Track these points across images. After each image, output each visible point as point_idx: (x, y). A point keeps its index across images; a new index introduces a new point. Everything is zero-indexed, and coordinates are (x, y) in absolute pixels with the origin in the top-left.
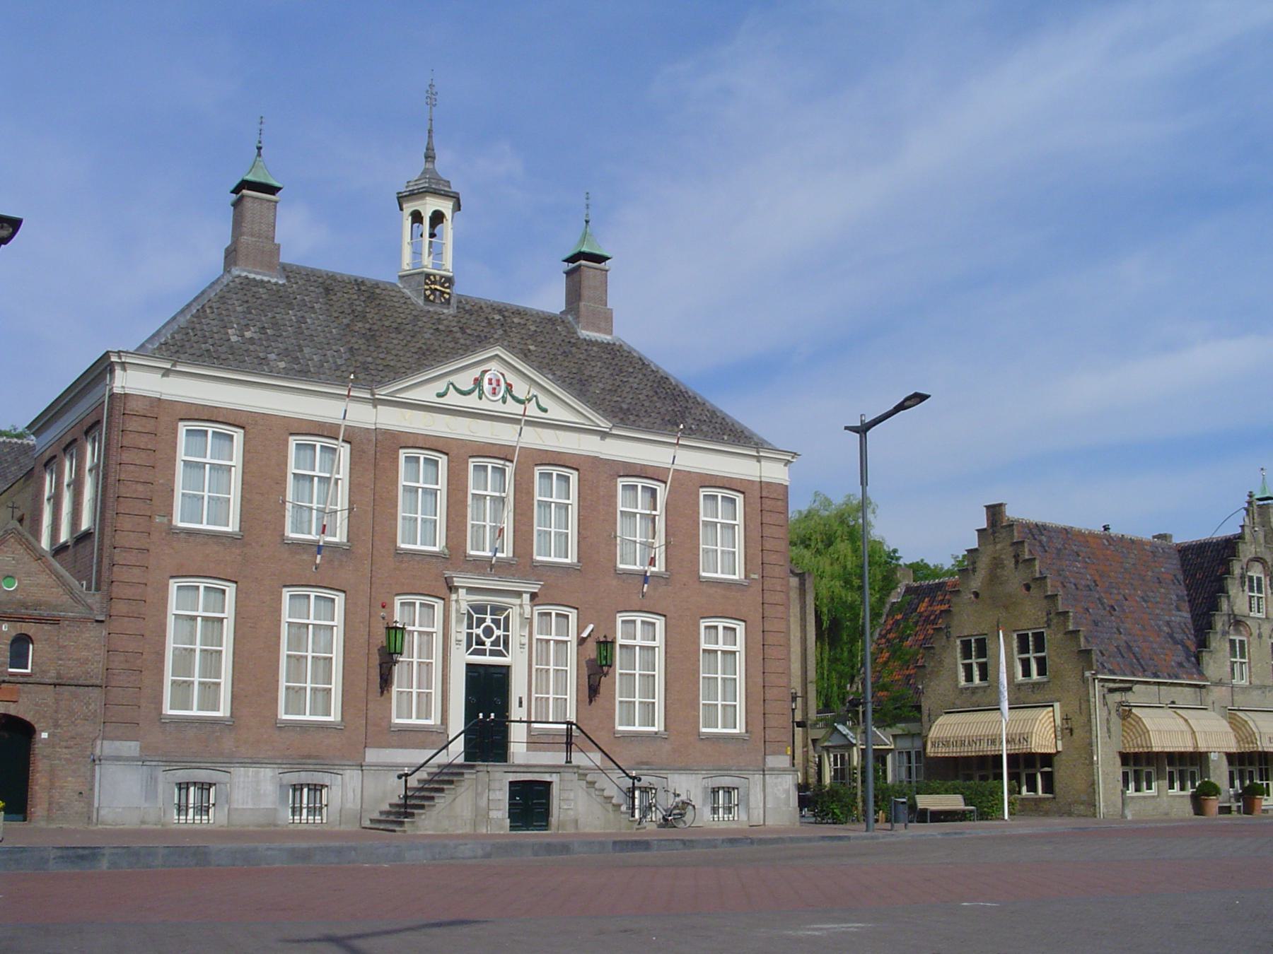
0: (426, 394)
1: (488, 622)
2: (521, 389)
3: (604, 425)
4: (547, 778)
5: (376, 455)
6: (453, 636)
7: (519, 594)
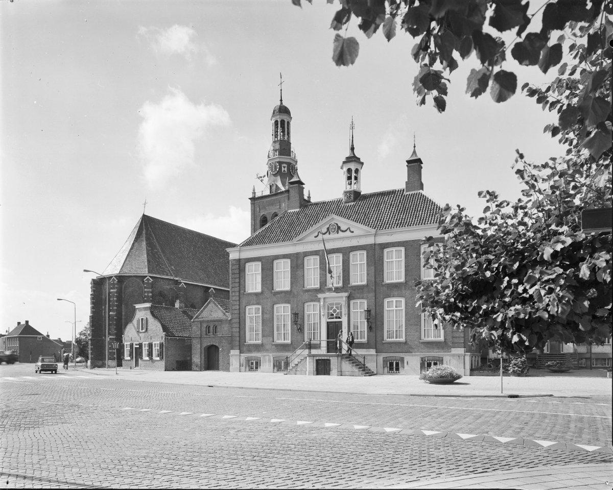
0: (312, 238)
1: (335, 308)
2: (343, 228)
3: (373, 231)
4: (328, 358)
5: (297, 262)
6: (322, 314)
7: (342, 297)
